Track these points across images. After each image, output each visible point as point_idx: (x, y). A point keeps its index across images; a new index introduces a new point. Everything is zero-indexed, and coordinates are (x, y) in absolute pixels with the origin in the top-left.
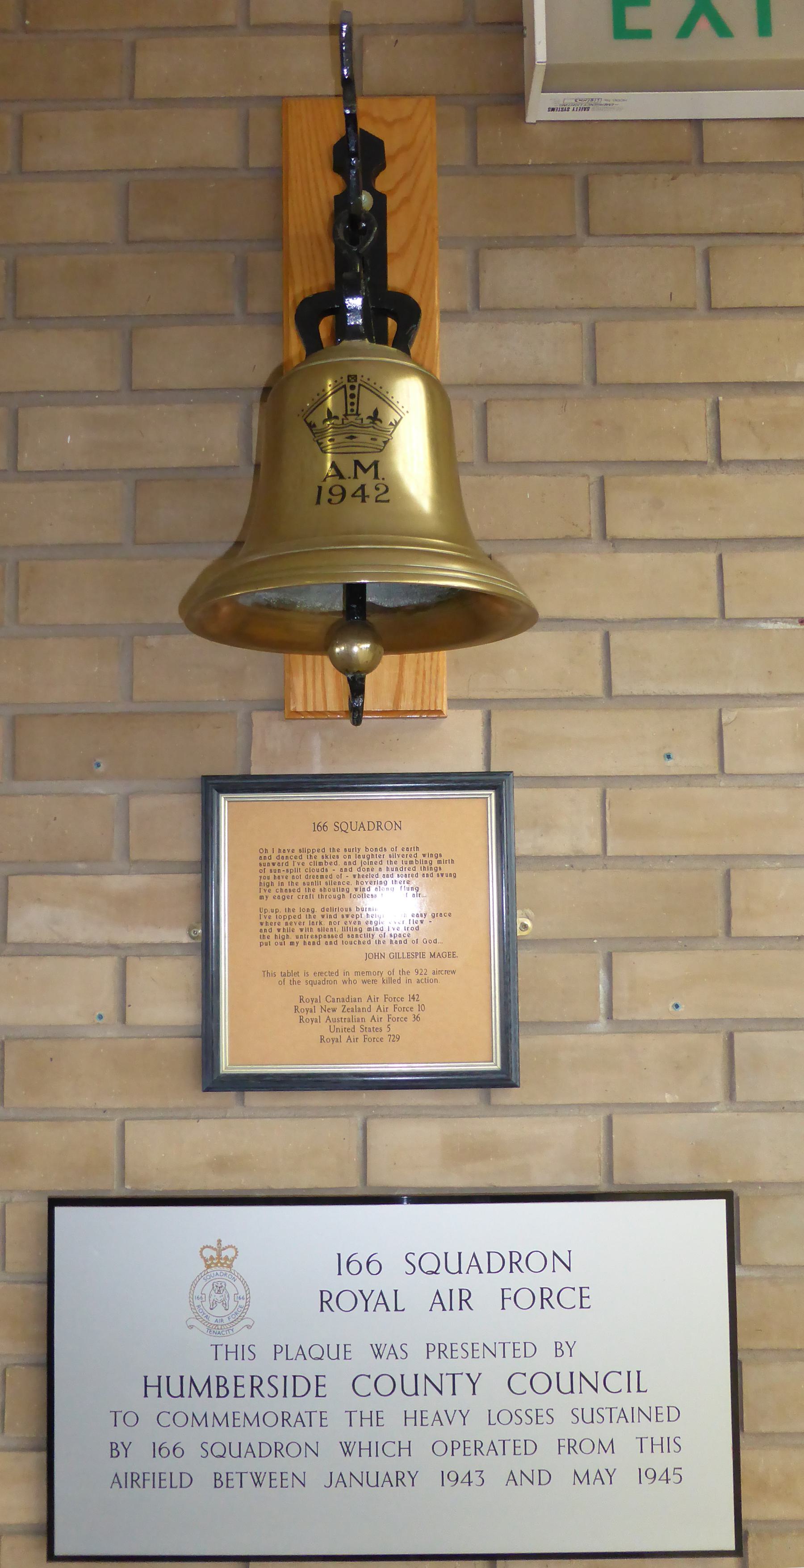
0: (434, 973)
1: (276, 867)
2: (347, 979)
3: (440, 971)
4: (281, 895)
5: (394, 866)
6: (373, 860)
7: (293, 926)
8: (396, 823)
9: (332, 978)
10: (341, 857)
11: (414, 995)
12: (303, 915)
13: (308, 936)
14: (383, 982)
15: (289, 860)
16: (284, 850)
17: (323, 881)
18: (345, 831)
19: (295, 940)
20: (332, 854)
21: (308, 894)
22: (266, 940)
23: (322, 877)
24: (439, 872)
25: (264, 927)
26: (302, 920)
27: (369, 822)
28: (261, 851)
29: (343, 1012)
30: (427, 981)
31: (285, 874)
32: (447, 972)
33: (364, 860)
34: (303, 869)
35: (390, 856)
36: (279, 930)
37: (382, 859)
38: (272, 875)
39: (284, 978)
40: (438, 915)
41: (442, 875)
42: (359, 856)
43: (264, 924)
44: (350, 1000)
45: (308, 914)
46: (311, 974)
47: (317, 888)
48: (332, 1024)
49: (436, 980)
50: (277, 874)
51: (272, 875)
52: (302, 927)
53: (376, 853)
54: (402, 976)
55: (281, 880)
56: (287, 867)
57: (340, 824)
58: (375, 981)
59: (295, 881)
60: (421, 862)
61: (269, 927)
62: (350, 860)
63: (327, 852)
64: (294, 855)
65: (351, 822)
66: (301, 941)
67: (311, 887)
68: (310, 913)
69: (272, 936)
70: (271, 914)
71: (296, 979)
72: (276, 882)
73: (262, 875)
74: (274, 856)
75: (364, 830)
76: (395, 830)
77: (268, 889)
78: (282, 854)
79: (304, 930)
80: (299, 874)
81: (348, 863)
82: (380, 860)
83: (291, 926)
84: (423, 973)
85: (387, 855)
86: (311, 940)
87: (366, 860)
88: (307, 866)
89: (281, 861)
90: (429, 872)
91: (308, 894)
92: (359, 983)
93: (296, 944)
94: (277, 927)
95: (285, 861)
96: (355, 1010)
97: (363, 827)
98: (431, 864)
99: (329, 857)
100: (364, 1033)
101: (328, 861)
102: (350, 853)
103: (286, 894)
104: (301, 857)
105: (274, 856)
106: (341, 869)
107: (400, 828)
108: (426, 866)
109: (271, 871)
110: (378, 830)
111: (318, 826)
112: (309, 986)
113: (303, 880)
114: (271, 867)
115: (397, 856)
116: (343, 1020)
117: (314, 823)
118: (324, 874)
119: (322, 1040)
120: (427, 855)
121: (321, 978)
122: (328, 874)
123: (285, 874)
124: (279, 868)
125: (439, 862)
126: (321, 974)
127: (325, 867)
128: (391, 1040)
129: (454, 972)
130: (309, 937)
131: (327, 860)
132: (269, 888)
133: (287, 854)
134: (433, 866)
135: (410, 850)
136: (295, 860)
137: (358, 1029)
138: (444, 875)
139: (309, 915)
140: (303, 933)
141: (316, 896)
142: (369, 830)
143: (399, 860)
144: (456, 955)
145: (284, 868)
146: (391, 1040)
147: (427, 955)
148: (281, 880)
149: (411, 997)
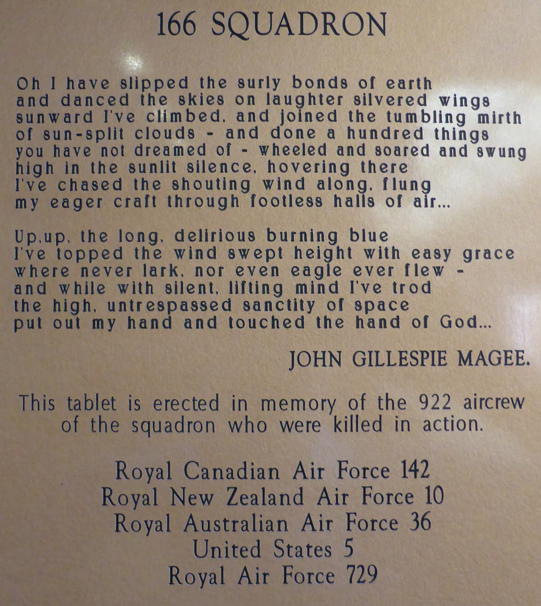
0: (468, 405)
1: (61, 126)
2: (240, 418)
3: (484, 401)
4: (71, 196)
5: (367, 126)
6: (314, 110)
7: (102, 279)
8: (371, 18)
9: (204, 416)
10: (229, 100)
11: (415, 463)
12: (128, 249)
13: (139, 303)
14: (336, 426)
15: (94, 108)
16: (82, 82)
17: (182, 161)
18: (240, 36)
19: (104, 315)
20: (206, 92)
21: (141, 195)
22: (32, 315)
23: (178, 150)
24: (483, 144)
25: (25, 280)
26: (124, 263)
27: (302, 14)
28: (23, 84)
29: (229, 504)
30: (449, 426)
31: (83, 143)
32: (501, 402)
33: (288, 109)
34: (129, 129)
35: (357, 100)
36: (64, 289)
37: (335, 106)
38: (48, 146)
39: (75, 413)
40: (481, 254)
41: (491, 151)
42: (277, 97)
43: (27, 272)
44: (249, 475)
45: (140, 246)
46: (147, 404)
47: (166, 179)
48: (201, 536)
49: (473, 424)
50: (62, 144)
51: (48, 146)
52: (123, 280)
53: (321, 91)
54: (384, 413)
55: (73, 159)
56: (88, 126)
57: (227, 16)
58: (313, 425)
59: (107, 161)
60: (437, 117)
61: (40, 279)
62: (252, 108)
63: (194, 88)
64: (106, 94)
65: (256, 14)
66: (121, 318)
67: (150, 177)
68: (147, 244)
69: (46, 302)
70: (45, 246)
71: (108, 416)
72: (59, 163)
73: (25, 144)
74: (55, 97)
75: (291, 33)
76: (371, 34)
77: (37, 181)
78: (75, 93)
79: (130, 289)
80: (118, 143)
81: (246, 117)
82: (331, 109)
83: (94, 279)
84: (440, 405)
85: (348, 95)
86: (148, 316)
87: (293, 108)
88: (140, 122)
89: (72, 110)
90: (458, 144)
91: (141, 195)
92: (274, 428)
93: (107, 325)
94: (60, 279)
95: (83, 110)
96: (250, 527)
97: (288, 25)
98: (463, 123)
99: (198, 100)
100: (285, 560)
101: (196, 110)
102: (251, 92)
103: (85, 196)
104: (125, 101)
105: (55, 97)
106: (230, 131)
107: (383, 32)
108: (449, 127)
109: (47, 135)
110: (325, 33)
111: (170, 22)
112: (142, 435)
113: (131, 157)
114: (48, 125)
115: (374, 100)
116: (230, 525)
117: (161, 15)
118: (185, 143)
119: (173, 576)
120: (451, 102)
121: (174, 416)
122: (196, 143)
123: (83, 143)
124: (67, 127)
125: (483, 119)
126: (171, 403)
127: (188, 126)
128: (355, 579)
129: (519, 403)
130: (143, 307)
131: (192, 108)
132: (41, 179)
133: (89, 91)
134: (468, 128)
135: (407, 85)
136: (109, 108)
137: (268, 549)
138: (496, 153)
139: (144, 250)
140: (127, 297)
141: (162, 201)
142: (302, 33)
143: (381, 111)
144: (526, 360)
145: (82, 127)
146: (355, 579)
147: (452, 358)
148: (73, 159)
149: (408, 467)
